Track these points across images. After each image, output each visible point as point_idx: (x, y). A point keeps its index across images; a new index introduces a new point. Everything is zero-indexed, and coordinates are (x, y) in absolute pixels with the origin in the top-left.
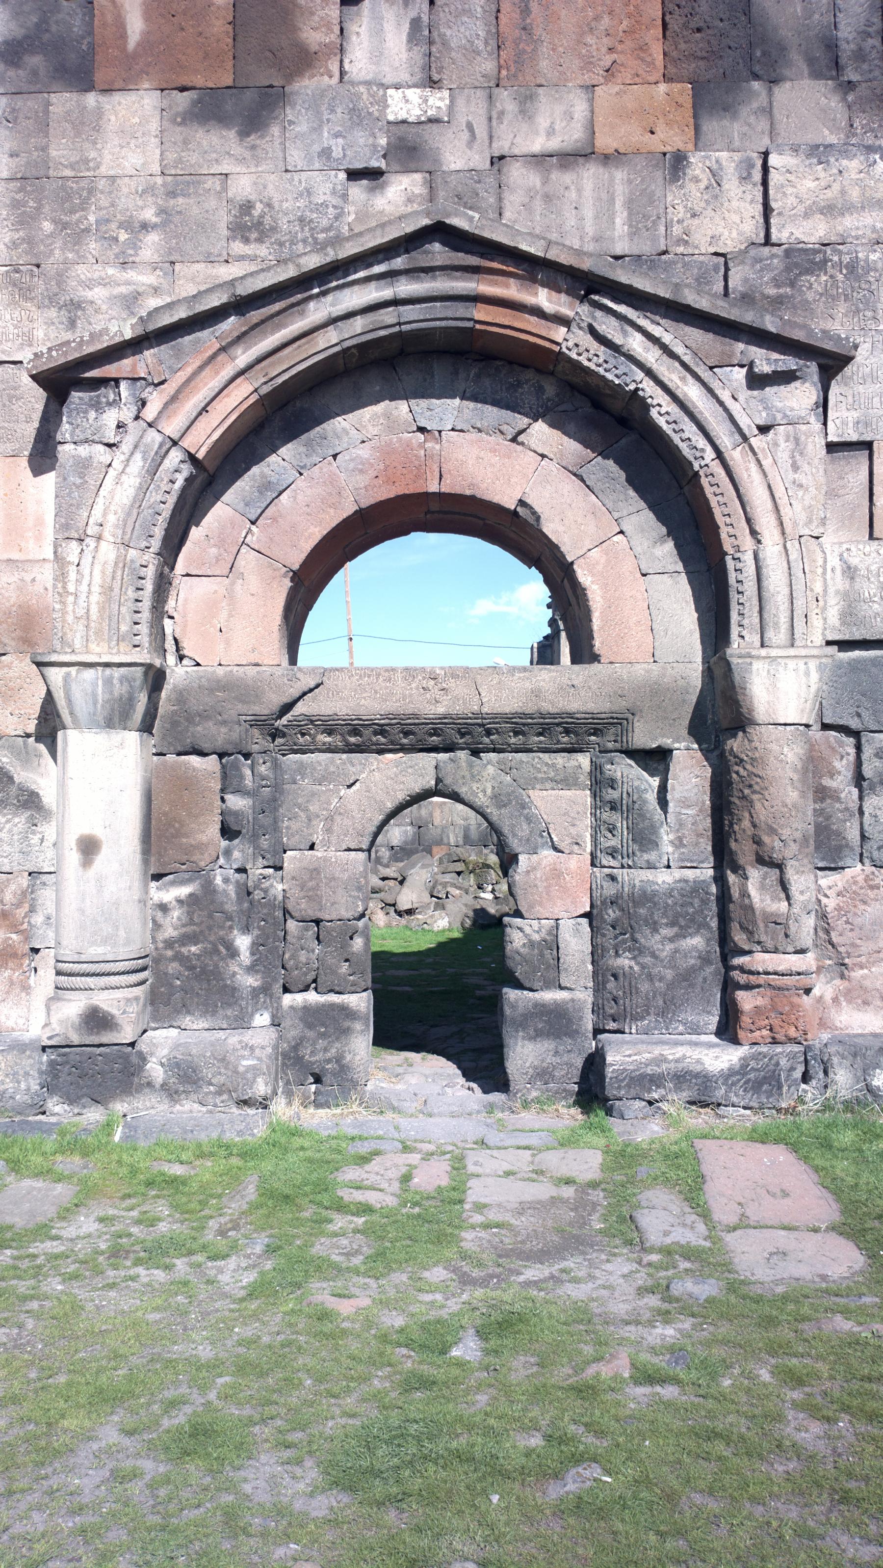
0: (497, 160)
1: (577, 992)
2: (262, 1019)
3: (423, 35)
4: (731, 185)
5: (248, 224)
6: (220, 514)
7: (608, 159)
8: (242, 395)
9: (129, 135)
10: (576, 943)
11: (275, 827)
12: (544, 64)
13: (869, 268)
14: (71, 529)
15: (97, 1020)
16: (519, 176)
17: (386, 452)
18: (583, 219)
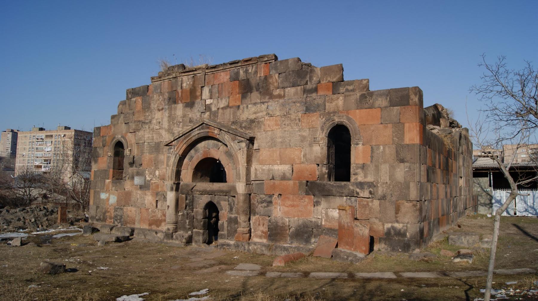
0: (218, 109)
1: (225, 232)
2: (190, 232)
3: (211, 92)
4: (245, 109)
5: (191, 121)
6: (186, 160)
7: (230, 108)
8: (185, 146)
9: (179, 109)
10: (226, 225)
11: (192, 205)
12: (224, 94)
13: (260, 121)
14: (167, 165)
15: (168, 229)
16: (220, 111)
17: (204, 152)
18: (225, 117)
